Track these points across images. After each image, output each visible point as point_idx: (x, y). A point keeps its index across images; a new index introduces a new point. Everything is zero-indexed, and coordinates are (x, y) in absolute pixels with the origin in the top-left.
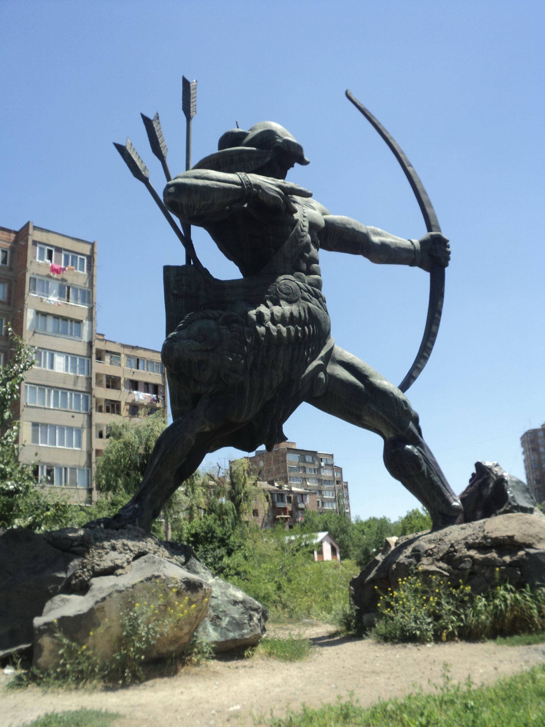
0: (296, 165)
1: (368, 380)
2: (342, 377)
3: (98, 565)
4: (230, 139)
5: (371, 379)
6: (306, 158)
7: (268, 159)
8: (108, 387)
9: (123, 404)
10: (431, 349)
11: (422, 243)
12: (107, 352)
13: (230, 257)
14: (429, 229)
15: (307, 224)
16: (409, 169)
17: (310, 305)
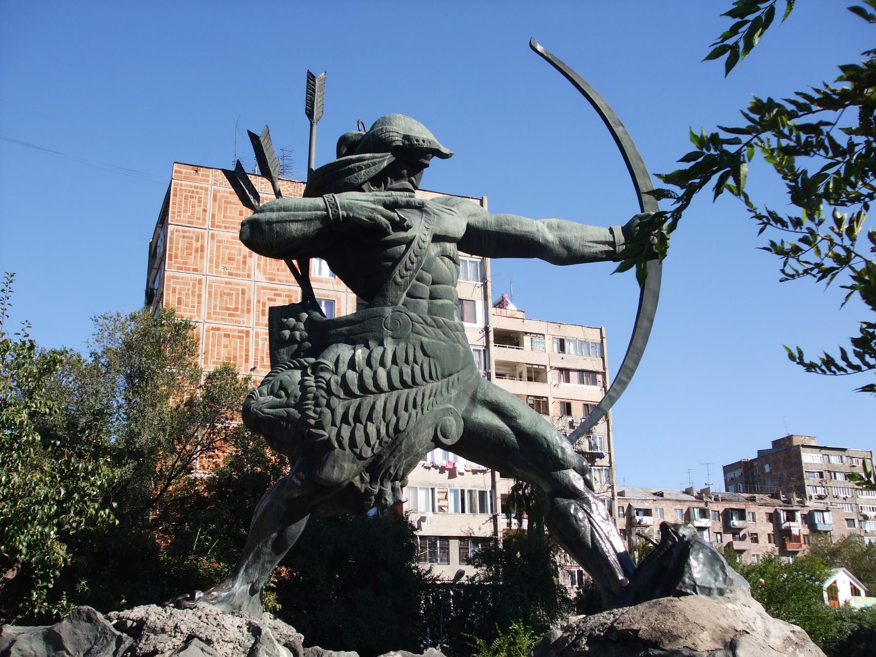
0: (434, 161)
1: (516, 422)
2: (482, 421)
3: (141, 649)
4: (347, 145)
5: (520, 421)
6: (444, 150)
7: (385, 164)
8: (530, 379)
9: (550, 401)
10: (633, 371)
11: (626, 230)
12: (526, 333)
14: (643, 211)
15: (429, 239)
16: (618, 130)
17: (425, 340)
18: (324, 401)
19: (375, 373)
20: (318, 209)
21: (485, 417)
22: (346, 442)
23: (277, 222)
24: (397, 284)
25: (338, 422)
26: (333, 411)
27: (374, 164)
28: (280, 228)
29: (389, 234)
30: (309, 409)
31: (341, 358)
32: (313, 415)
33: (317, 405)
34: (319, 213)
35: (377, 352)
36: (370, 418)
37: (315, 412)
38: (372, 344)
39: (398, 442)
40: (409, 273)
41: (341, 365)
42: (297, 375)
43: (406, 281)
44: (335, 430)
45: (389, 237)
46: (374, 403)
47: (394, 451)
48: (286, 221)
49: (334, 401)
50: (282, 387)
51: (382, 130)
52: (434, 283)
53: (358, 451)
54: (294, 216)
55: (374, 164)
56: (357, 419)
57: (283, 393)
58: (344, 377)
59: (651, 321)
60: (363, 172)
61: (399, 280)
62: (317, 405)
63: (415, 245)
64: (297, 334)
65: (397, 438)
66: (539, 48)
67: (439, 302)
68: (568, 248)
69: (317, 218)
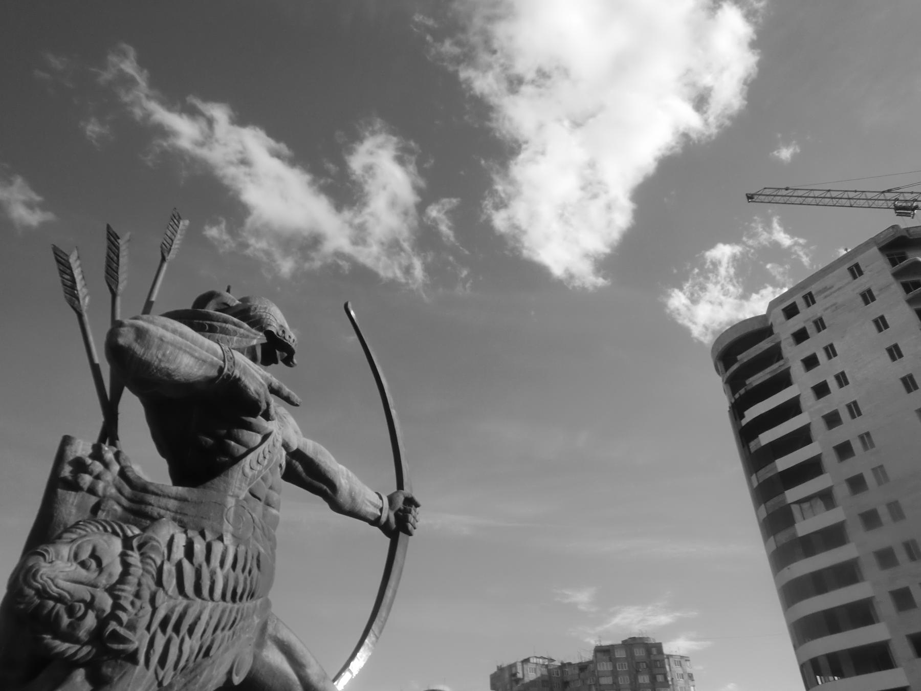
2: (272, 661)
13: (163, 453)
17: (262, 550)
18: (146, 594)
19: (213, 574)
20: (215, 353)
21: (275, 658)
22: (155, 659)
23: (172, 345)
24: (244, 474)
25: (153, 629)
26: (155, 609)
27: (247, 337)
28: (171, 353)
29: (255, 416)
30: (126, 598)
31: (176, 540)
32: (129, 607)
33: (137, 595)
34: (215, 359)
35: (218, 548)
36: (191, 631)
37: (132, 603)
38: (209, 536)
39: (198, 671)
40: (259, 468)
41: (174, 549)
42: (117, 545)
43: (254, 476)
44: (147, 637)
45: (252, 420)
46: (201, 613)
47: (189, 682)
48: (180, 349)
49: (161, 595)
50: (94, 555)
51: (266, 308)
52: (271, 488)
53: (161, 674)
54: (191, 348)
55: (247, 337)
56: (177, 629)
57: (93, 564)
58: (179, 566)
59: (395, 592)
60: (235, 338)
61: (247, 470)
62: (137, 595)
63: (270, 439)
64: (101, 486)
65: (200, 664)
66: (352, 313)
67: (274, 511)
68: (353, 499)
69: (212, 364)
